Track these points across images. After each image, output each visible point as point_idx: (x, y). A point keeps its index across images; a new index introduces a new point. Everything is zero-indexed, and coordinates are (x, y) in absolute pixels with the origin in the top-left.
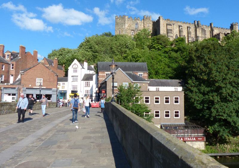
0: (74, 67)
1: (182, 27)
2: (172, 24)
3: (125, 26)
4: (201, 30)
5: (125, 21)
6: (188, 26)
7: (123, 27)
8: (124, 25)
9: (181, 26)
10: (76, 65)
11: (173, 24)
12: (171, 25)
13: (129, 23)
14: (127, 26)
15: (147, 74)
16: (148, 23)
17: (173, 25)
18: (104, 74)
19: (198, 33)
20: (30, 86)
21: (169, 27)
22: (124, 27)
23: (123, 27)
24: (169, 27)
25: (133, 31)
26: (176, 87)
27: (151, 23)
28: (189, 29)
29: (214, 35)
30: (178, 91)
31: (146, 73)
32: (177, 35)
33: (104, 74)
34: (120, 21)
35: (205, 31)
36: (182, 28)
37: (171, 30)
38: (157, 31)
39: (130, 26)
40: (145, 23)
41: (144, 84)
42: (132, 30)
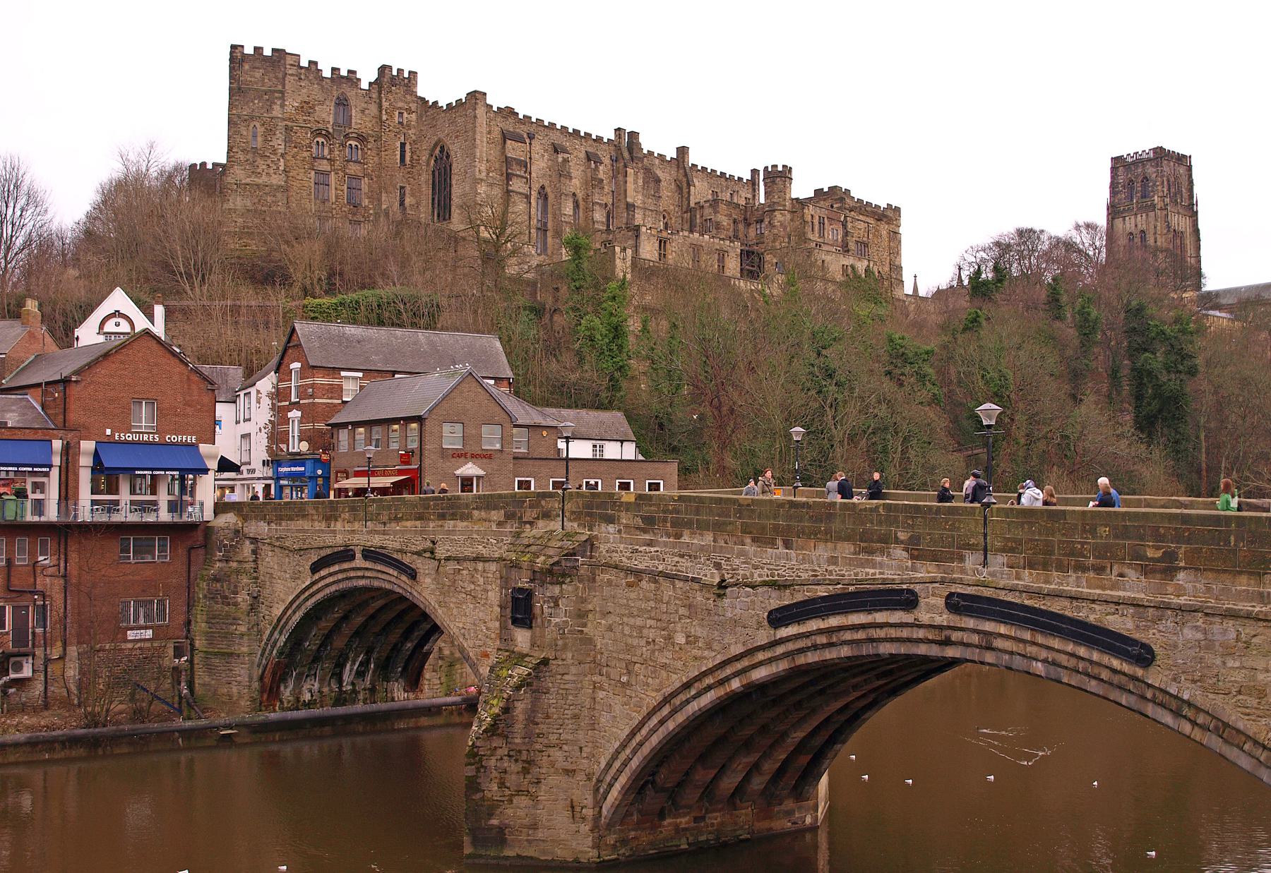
0: (110, 327)
1: (566, 156)
2: (525, 136)
3: (282, 106)
4: (641, 175)
5: (284, 79)
6: (590, 150)
7: (275, 113)
8: (279, 103)
9: (565, 151)
10: (123, 322)
11: (531, 137)
12: (519, 139)
13: (304, 91)
14: (292, 103)
15: (510, 384)
16: (400, 104)
17: (528, 141)
18: (336, 381)
19: (630, 186)
20: (108, 432)
21: (515, 150)
22: (277, 111)
23: (275, 113)
24: (515, 150)
25: (321, 140)
26: (598, 443)
27: (413, 109)
28: (597, 167)
29: (692, 205)
30: (606, 457)
31: (505, 383)
32: (543, 187)
33: (336, 381)
34: (258, 74)
35: (658, 181)
36: (566, 161)
37: (524, 165)
38: (448, 156)
39: (307, 108)
40: (385, 104)
41: (545, 433)
42: (320, 134)
